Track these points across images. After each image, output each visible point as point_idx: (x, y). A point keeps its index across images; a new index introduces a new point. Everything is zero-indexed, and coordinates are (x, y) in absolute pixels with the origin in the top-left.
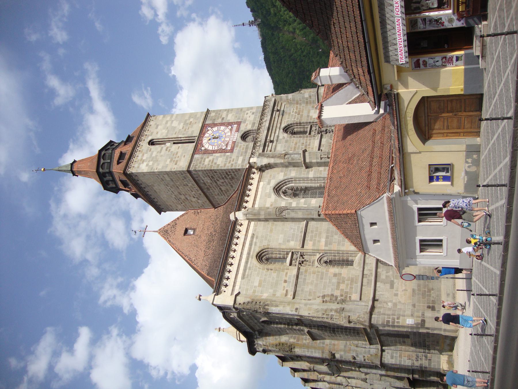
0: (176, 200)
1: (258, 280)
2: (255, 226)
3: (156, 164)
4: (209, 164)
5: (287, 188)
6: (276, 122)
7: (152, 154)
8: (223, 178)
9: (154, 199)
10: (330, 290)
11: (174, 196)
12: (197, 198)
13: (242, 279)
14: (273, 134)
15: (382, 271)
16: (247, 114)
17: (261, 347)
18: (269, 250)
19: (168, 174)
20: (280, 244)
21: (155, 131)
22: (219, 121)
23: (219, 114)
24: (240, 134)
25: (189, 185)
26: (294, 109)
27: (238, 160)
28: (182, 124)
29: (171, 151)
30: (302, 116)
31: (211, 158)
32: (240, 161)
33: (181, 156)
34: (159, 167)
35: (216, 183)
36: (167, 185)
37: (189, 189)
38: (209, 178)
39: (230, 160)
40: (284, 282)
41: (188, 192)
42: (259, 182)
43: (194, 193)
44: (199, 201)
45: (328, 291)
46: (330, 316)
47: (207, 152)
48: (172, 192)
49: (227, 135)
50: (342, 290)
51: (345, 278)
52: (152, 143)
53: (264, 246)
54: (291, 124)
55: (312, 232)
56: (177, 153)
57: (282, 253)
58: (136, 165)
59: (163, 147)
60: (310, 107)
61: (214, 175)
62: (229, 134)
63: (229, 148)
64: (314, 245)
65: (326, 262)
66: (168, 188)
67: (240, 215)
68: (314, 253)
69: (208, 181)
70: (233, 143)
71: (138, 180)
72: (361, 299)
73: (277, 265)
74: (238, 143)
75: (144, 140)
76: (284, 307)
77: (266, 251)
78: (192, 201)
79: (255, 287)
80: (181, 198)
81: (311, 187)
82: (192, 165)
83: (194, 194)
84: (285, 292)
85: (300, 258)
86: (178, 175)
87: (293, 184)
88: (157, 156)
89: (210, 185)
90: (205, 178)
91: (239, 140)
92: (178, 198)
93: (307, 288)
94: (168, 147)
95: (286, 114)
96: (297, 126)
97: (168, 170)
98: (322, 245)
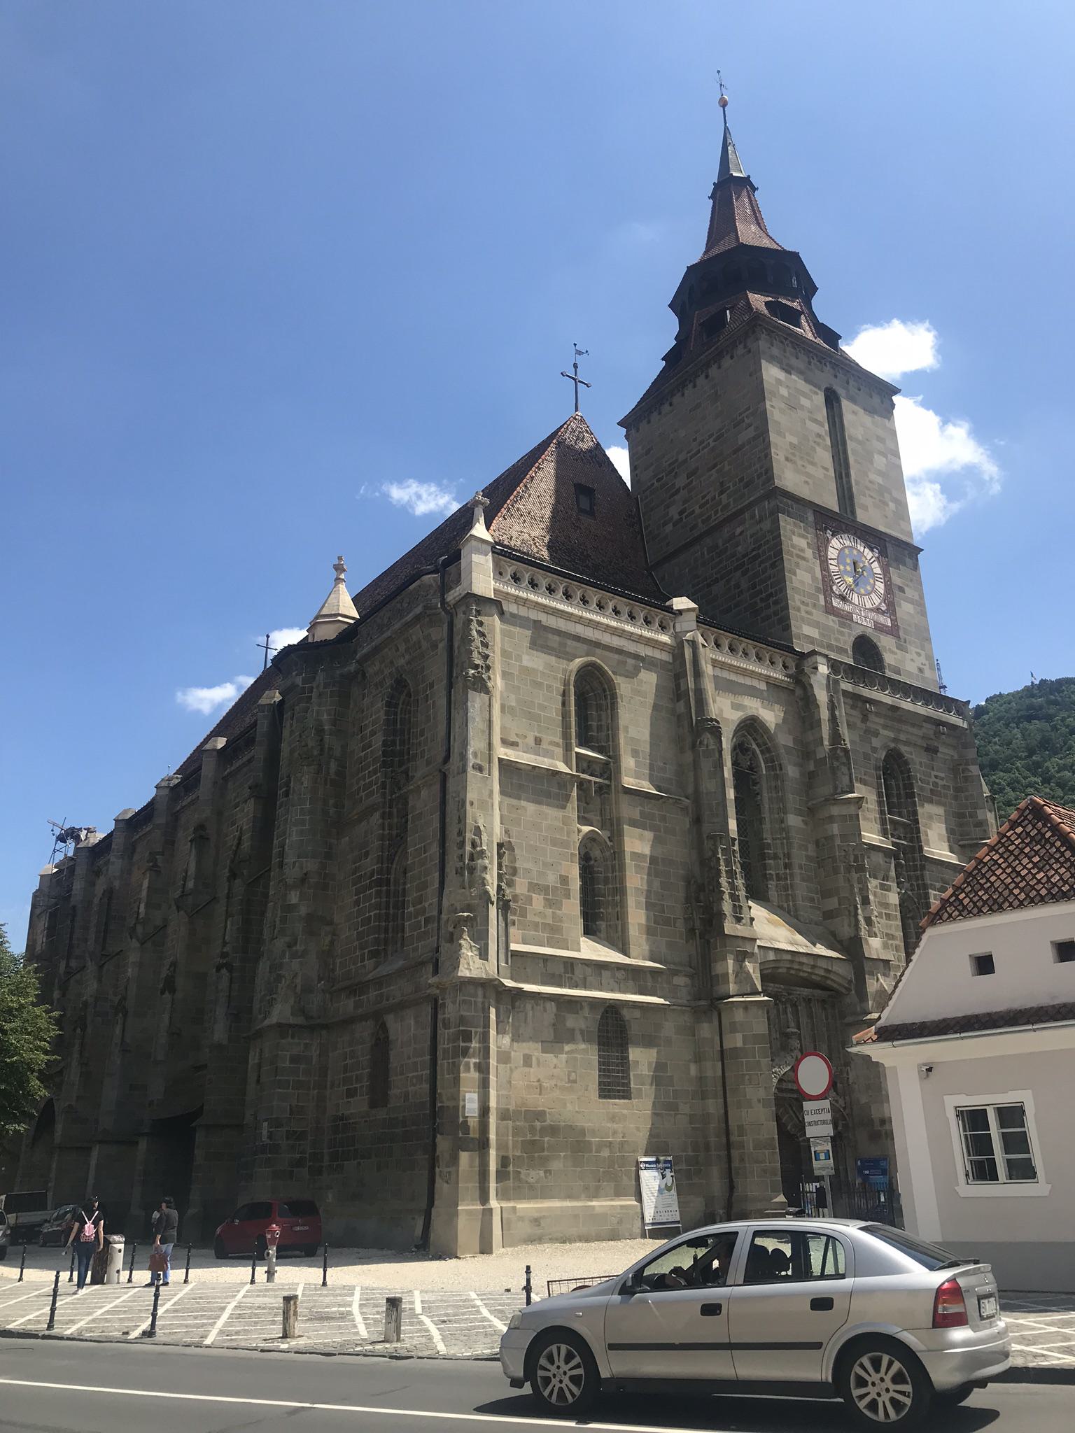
0: (670, 465)
1: (535, 667)
2: (664, 664)
3: (783, 405)
4: (793, 546)
5: (754, 753)
6: (910, 729)
8: (754, 586)
9: (671, 405)
10: (526, 866)
11: (681, 457)
12: (681, 519)
13: (535, 621)
14: (882, 721)
15: (586, 1018)
16: (919, 654)
17: (304, 681)
18: (609, 701)
19: (754, 438)
20: (626, 728)
23: (911, 581)
24: (870, 633)
25: (724, 496)
26: (942, 779)
27: (809, 625)
28: (879, 480)
29: (818, 449)
31: (809, 553)
32: (808, 630)
33: (808, 475)
34: (776, 412)
35: (736, 569)
36: (718, 438)
37: (708, 497)
38: (750, 550)
39: (807, 605)
40: (536, 738)
41: (700, 496)
42: (768, 680)
43: (698, 511)
44: (669, 528)
45: (523, 862)
46: (471, 863)
48: (698, 452)
49: (866, 598)
50: (529, 900)
51: (560, 909)
52: (832, 400)
53: (619, 684)
54: (909, 771)
55: (663, 819)
56: (813, 464)
57: (604, 734)
59: (823, 427)
61: (762, 562)
62: (869, 605)
63: (836, 603)
66: (712, 439)
68: (612, 825)
69: (740, 548)
70: (849, 613)
71: (732, 357)
72: (516, 954)
74: (850, 627)
75: (836, 376)
76: (483, 731)
77: (604, 690)
78: (668, 507)
79: (519, 658)
80: (675, 477)
81: (761, 821)
82: (790, 502)
83: (693, 511)
84: (513, 738)
85: (595, 783)
86: (757, 466)
87: (764, 773)
88: (802, 407)
89: (728, 553)
90: (751, 537)
91: (858, 631)
92: (676, 470)
94: (824, 440)
95: (930, 757)
96: (905, 789)
97: (773, 437)
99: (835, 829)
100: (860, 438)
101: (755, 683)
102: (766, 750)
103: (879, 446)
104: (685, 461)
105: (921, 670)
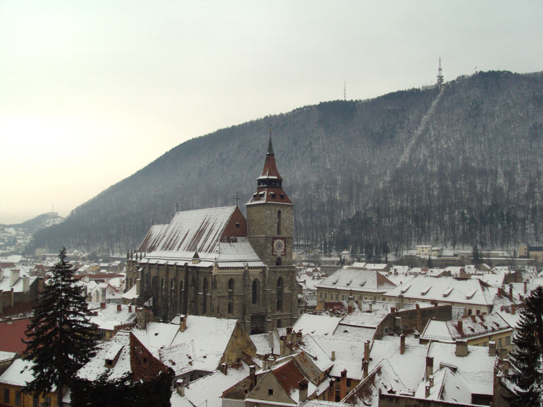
2: (242, 275)
22: (287, 245)
28: (287, 225)
31: (270, 246)
42: (259, 272)
45: (220, 308)
47: (273, 243)
56: (273, 228)
58: (269, 208)
62: (280, 251)
63: (274, 253)
73: (228, 286)
88: (272, 217)
98: (236, 302)
99: (266, 294)
100: (284, 218)
101: (257, 273)
102: (258, 282)
103: (288, 218)
104: (254, 221)
105: (289, 260)
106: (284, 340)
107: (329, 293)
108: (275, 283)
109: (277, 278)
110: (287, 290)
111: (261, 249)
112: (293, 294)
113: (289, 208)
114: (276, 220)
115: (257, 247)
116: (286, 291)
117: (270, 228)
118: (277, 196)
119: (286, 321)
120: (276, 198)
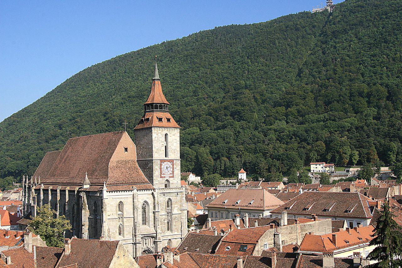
6: (172, 194)
7: (160, 138)
20: (125, 209)
21: (171, 135)
22: (175, 167)
28: (174, 148)
30: (175, 204)
31: (158, 168)
42: (148, 194)
47: (161, 165)
58: (156, 131)
60: (179, 207)
63: (162, 175)
64: (126, 221)
65: (120, 226)
67: (135, 191)
73: (118, 209)
91: (166, 179)
93: (111, 223)
100: (171, 141)
106: (160, 258)
107: (219, 212)
108: (165, 204)
109: (166, 199)
110: (177, 210)
111: (150, 172)
112: (182, 215)
113: (176, 131)
114: (163, 143)
115: (146, 170)
116: (175, 211)
117: (158, 152)
118: (163, 119)
119: (176, 240)
120: (163, 122)
